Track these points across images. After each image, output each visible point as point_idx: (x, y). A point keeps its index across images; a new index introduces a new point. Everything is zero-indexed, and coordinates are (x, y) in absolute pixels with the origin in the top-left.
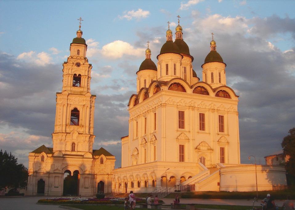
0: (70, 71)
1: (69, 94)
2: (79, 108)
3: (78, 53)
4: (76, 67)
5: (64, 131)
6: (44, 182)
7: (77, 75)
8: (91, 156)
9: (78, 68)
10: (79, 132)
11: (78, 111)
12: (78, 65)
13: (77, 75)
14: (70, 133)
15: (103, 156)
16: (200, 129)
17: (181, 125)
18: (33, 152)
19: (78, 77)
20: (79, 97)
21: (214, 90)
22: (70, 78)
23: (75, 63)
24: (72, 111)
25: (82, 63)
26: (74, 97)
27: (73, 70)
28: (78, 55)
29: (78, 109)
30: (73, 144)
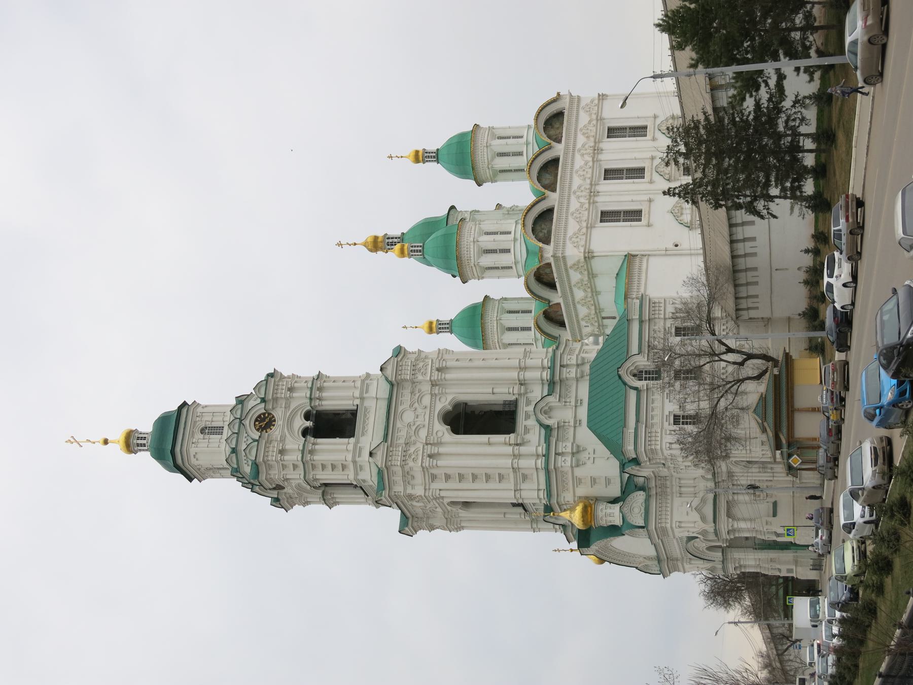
2: (444, 404)
3: (218, 430)
4: (276, 432)
7: (309, 424)
9: (279, 422)
10: (546, 393)
12: (265, 422)
13: (309, 424)
19: (315, 422)
20: (400, 408)
23: (256, 435)
25: (261, 409)
26: (399, 424)
28: (226, 428)
29: (450, 408)
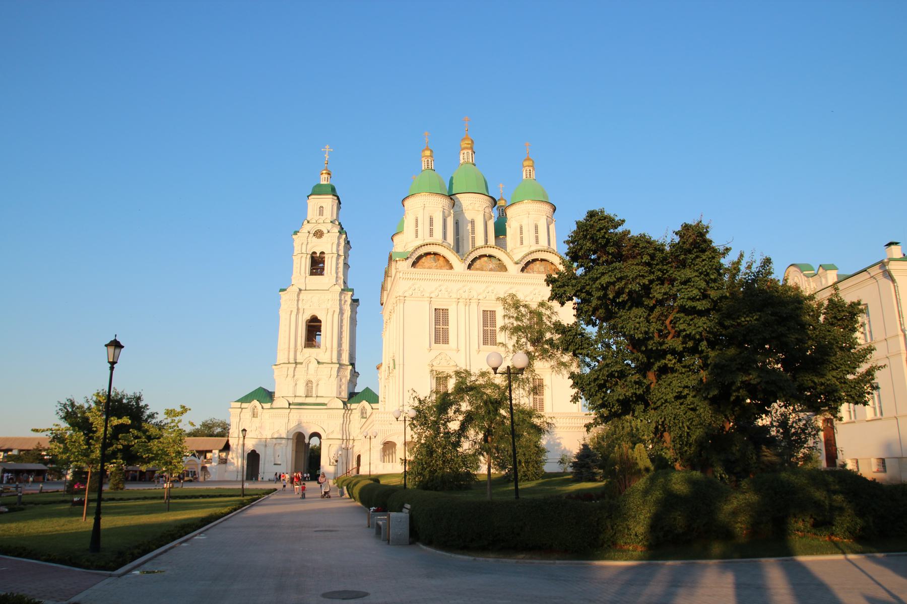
1: (300, 290)
4: (314, 239)
5: (292, 361)
6: (258, 455)
8: (341, 405)
11: (320, 321)
14: (301, 363)
18: (238, 401)
22: (303, 260)
25: (325, 231)
30: (309, 383)
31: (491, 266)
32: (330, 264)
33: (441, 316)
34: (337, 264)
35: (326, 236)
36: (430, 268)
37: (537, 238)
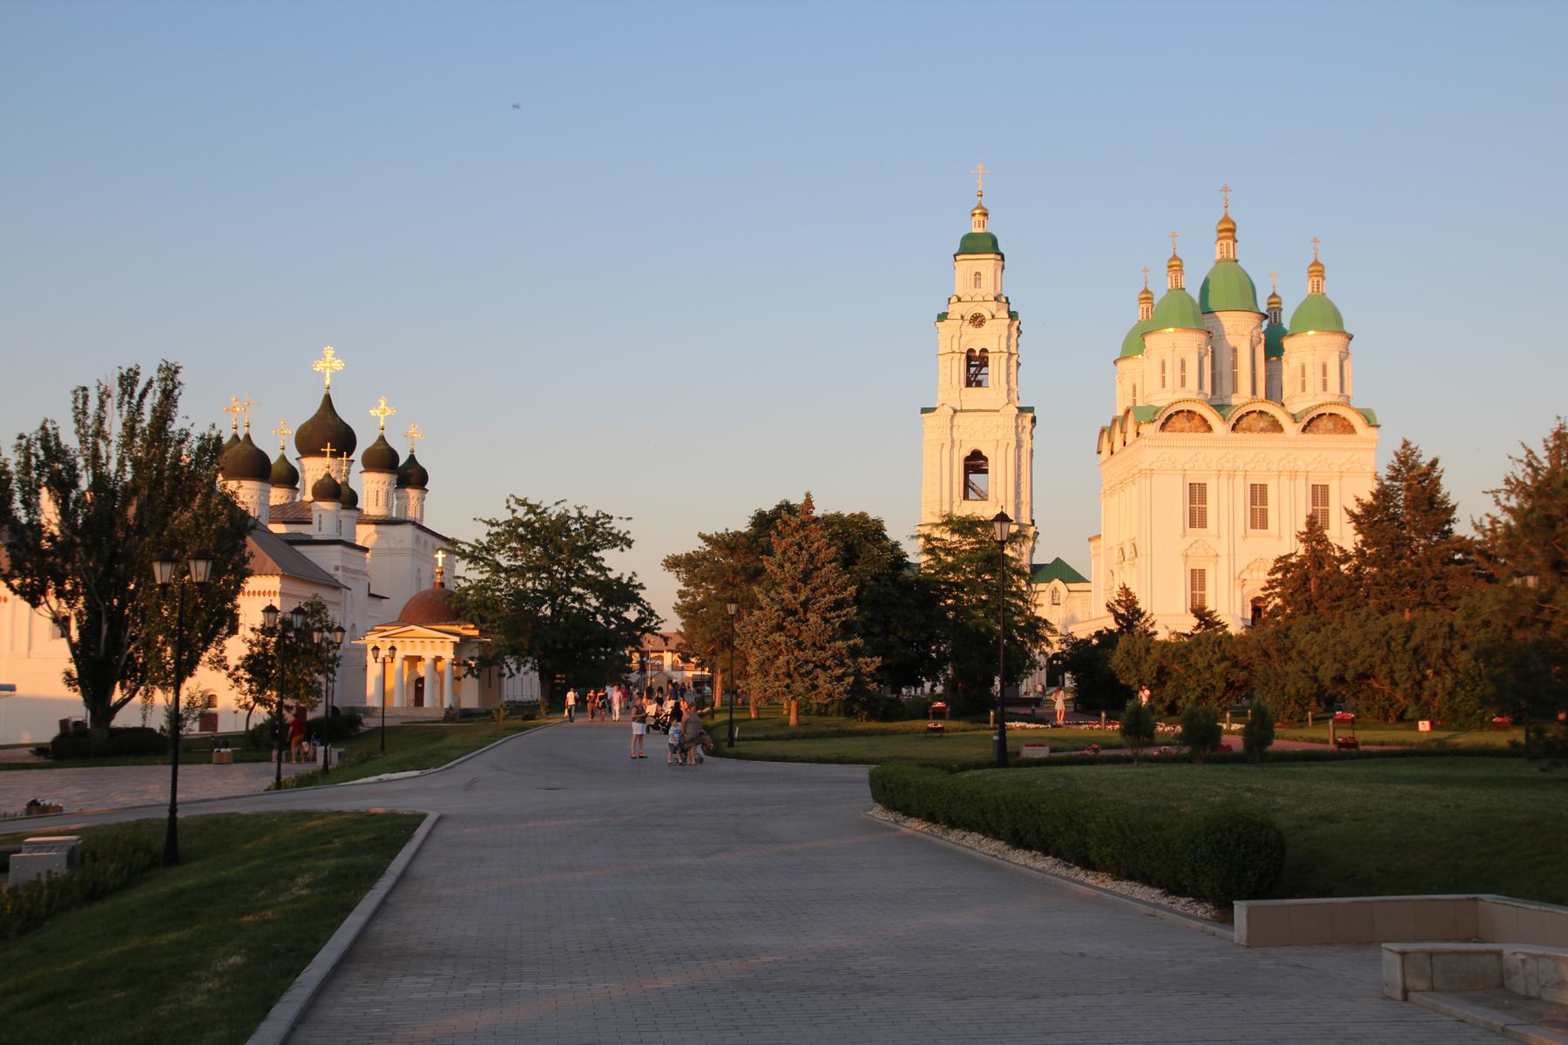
0: (956, 341)
4: (971, 329)
11: (986, 459)
12: (977, 320)
15: (1057, 583)
16: (1253, 526)
17: (1197, 518)
21: (1295, 418)
22: (955, 362)
23: (968, 317)
24: (967, 459)
25: (988, 316)
27: (963, 340)
31: (1262, 425)
32: (996, 369)
33: (1197, 493)
34: (1008, 367)
35: (988, 324)
36: (1182, 431)
37: (1325, 382)
